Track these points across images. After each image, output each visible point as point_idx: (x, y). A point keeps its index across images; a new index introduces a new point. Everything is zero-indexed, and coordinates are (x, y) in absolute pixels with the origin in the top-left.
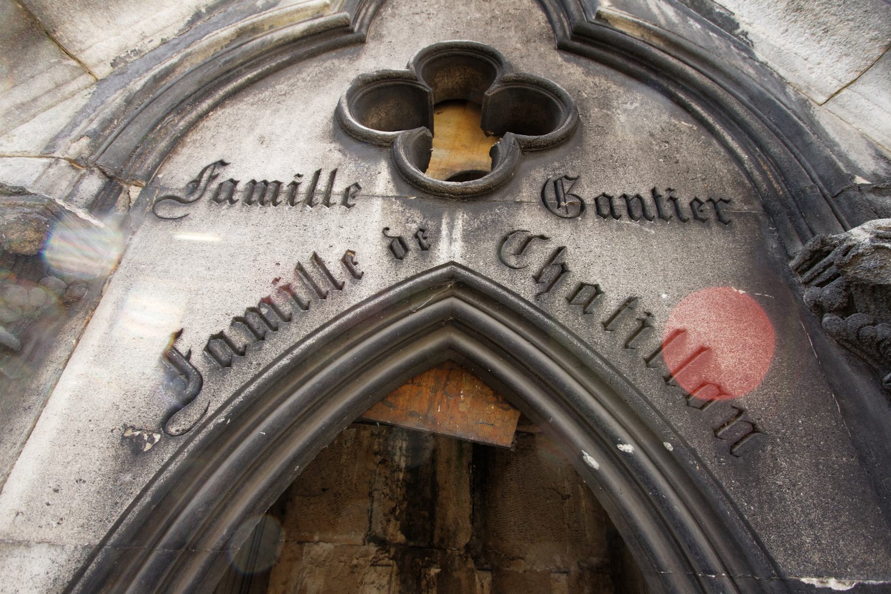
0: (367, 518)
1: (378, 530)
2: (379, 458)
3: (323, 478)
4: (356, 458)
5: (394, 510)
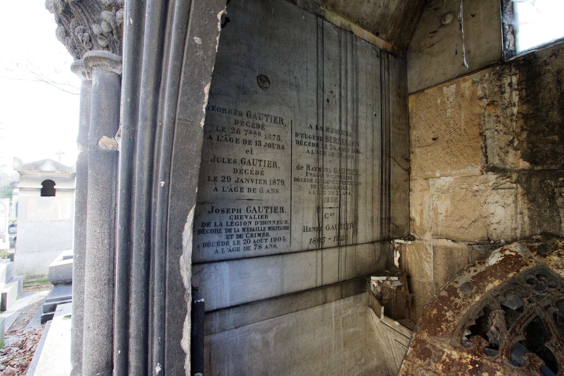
0: (481, 154)
1: (495, 161)
3: (434, 132)
4: (460, 109)
5: (512, 142)
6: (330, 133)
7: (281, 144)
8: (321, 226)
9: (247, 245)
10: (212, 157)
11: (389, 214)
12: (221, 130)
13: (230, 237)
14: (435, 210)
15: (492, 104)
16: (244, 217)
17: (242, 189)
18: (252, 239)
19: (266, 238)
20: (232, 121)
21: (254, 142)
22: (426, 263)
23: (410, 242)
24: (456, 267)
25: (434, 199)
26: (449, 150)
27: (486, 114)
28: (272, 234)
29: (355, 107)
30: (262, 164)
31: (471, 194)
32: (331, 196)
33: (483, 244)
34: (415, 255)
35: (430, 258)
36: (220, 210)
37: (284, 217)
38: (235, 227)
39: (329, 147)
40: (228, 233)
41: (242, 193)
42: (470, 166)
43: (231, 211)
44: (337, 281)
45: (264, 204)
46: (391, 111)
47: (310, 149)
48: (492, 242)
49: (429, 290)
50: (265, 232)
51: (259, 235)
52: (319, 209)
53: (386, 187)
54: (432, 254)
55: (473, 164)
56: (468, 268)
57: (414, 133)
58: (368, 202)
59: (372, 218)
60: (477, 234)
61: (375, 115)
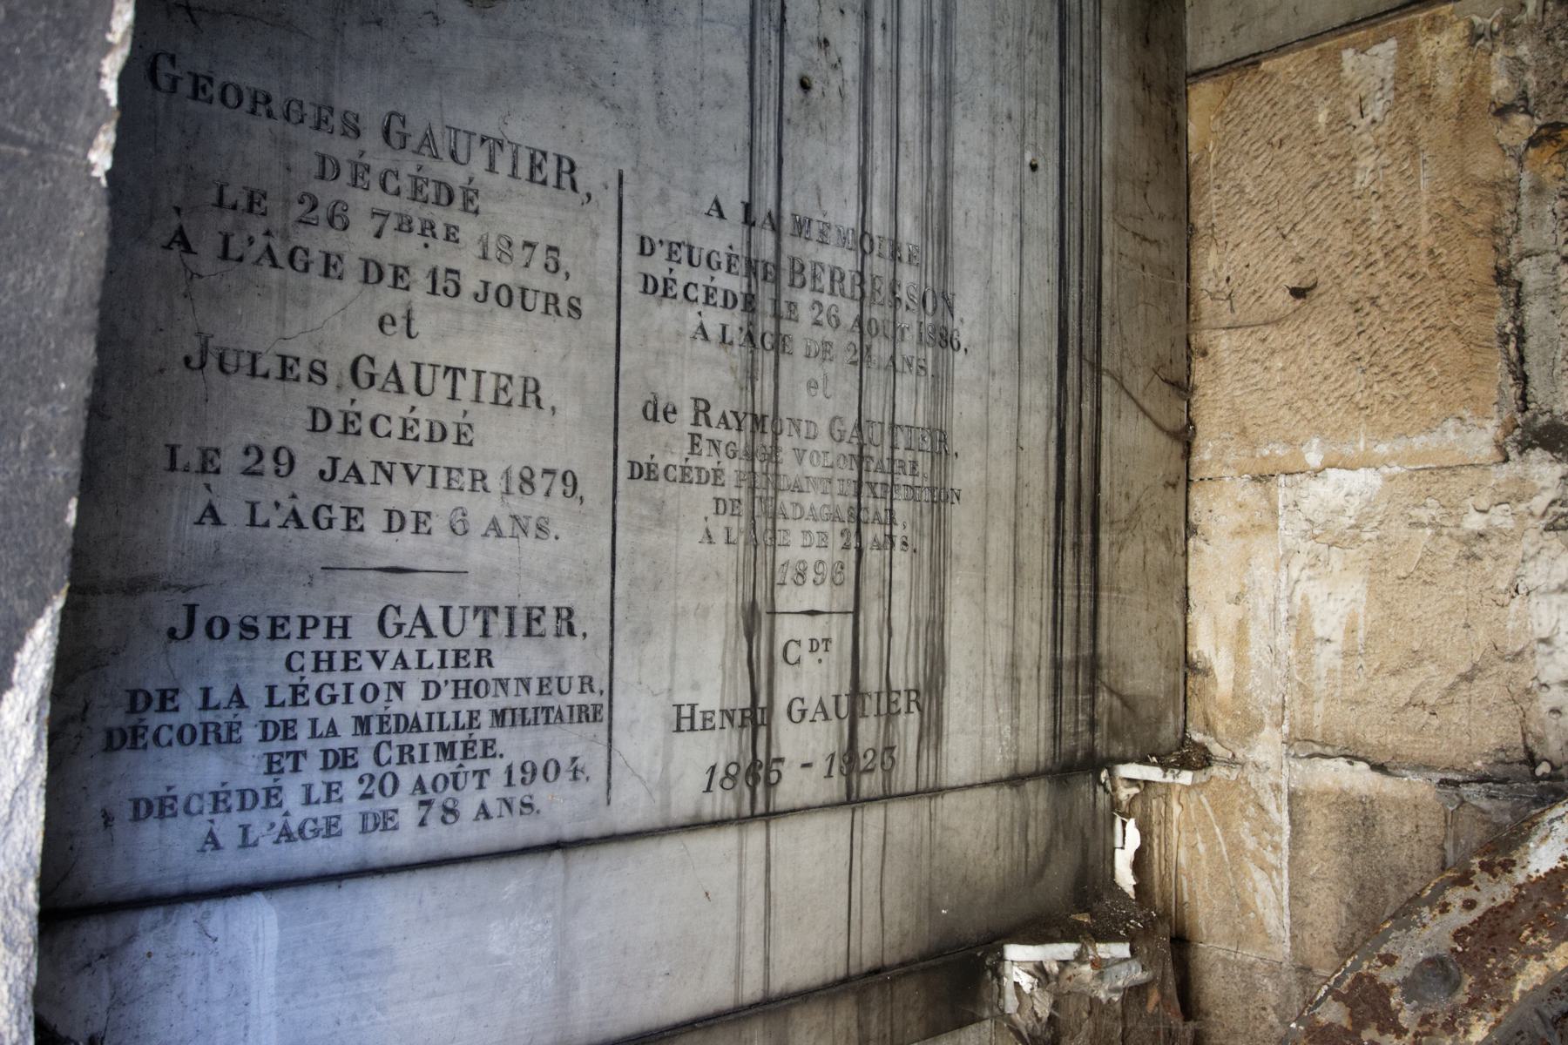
0: (1500, 365)
2: (1522, 126)
3: (1298, 260)
4: (1415, 153)
6: (811, 247)
7: (565, 291)
8: (762, 702)
9: (380, 804)
10: (192, 347)
11: (1094, 645)
12: (243, 203)
13: (288, 764)
14: (1300, 622)
15: (1549, 138)
16: (366, 660)
17: (353, 516)
18: (407, 775)
19: (480, 764)
20: (305, 162)
21: (420, 277)
22: (1258, 875)
23: (1186, 777)
24: (1390, 888)
25: (1295, 573)
26: (1361, 345)
27: (1525, 185)
28: (515, 745)
29: (937, 123)
30: (466, 387)
31: (1455, 550)
32: (812, 555)
33: (1504, 781)
34: (1210, 839)
35: (1276, 848)
36: (234, 620)
37: (576, 658)
38: (314, 710)
39: (805, 315)
40: (277, 746)
41: (355, 537)
42: (1451, 423)
43: (294, 627)
44: (841, 973)
45: (474, 595)
46: (1107, 149)
47: (714, 319)
48: (1543, 769)
49: (1273, 1000)
50: (478, 735)
51: (446, 750)
52: (754, 619)
53: (1079, 514)
54: (1287, 828)
55: (1466, 414)
56: (1440, 890)
57: (1212, 259)
58: (991, 586)
59: (1014, 663)
60: (1480, 733)
61: (1034, 167)
